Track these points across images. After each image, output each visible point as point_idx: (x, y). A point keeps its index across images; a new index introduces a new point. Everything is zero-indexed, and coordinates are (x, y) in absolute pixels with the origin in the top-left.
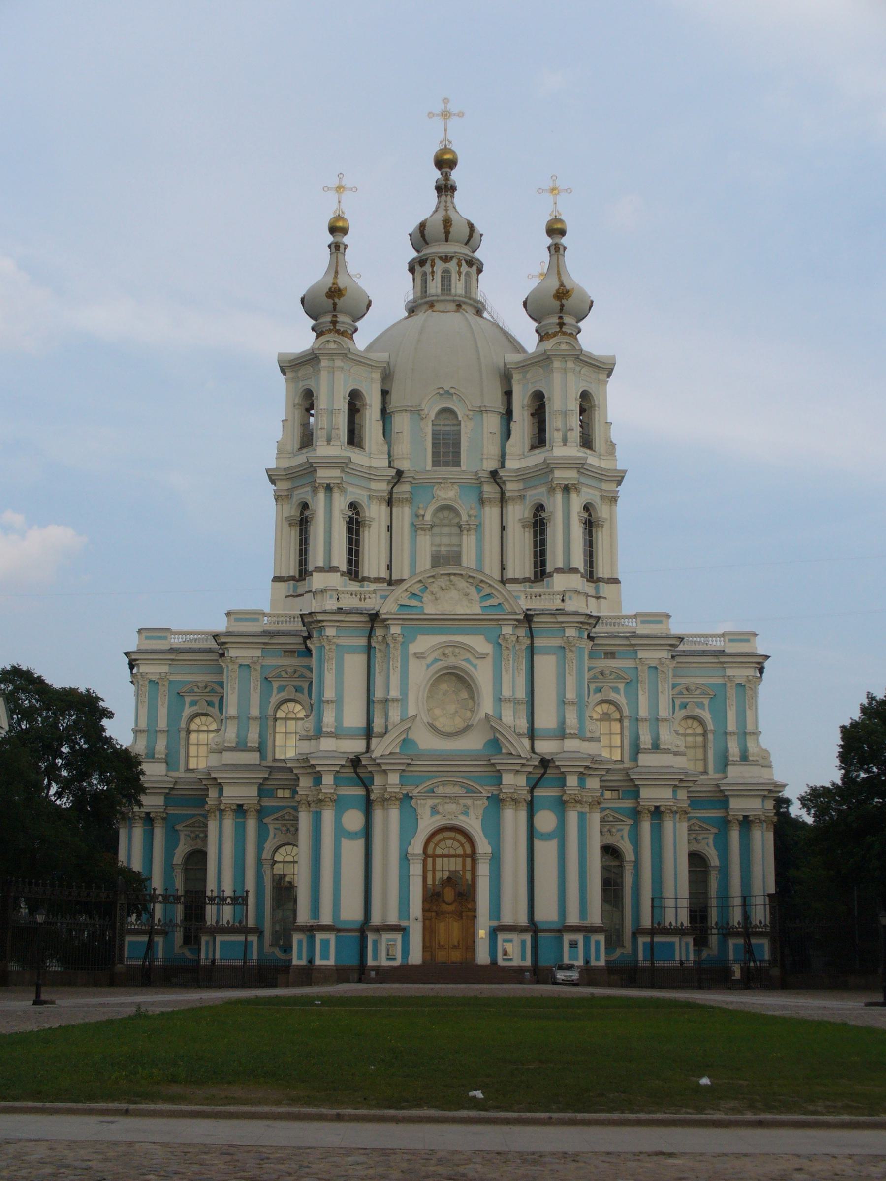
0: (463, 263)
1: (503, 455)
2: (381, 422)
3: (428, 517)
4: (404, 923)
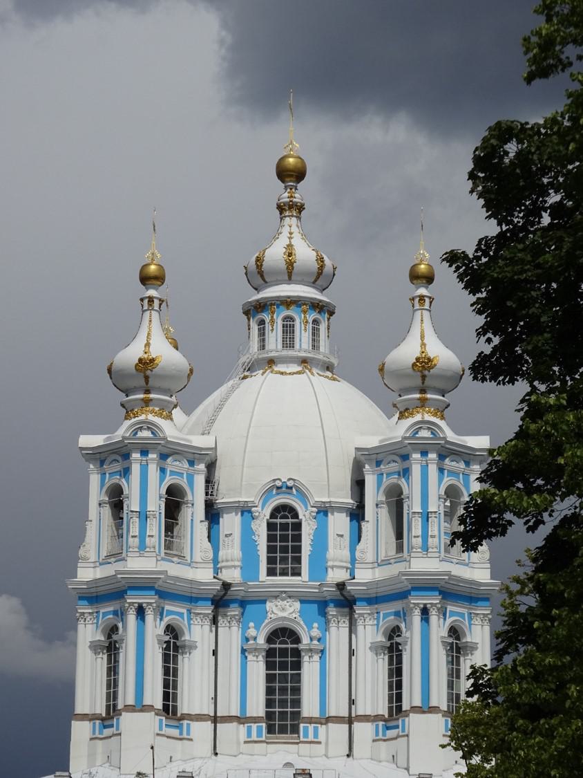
1: (353, 560)
2: (207, 523)
3: (261, 640)
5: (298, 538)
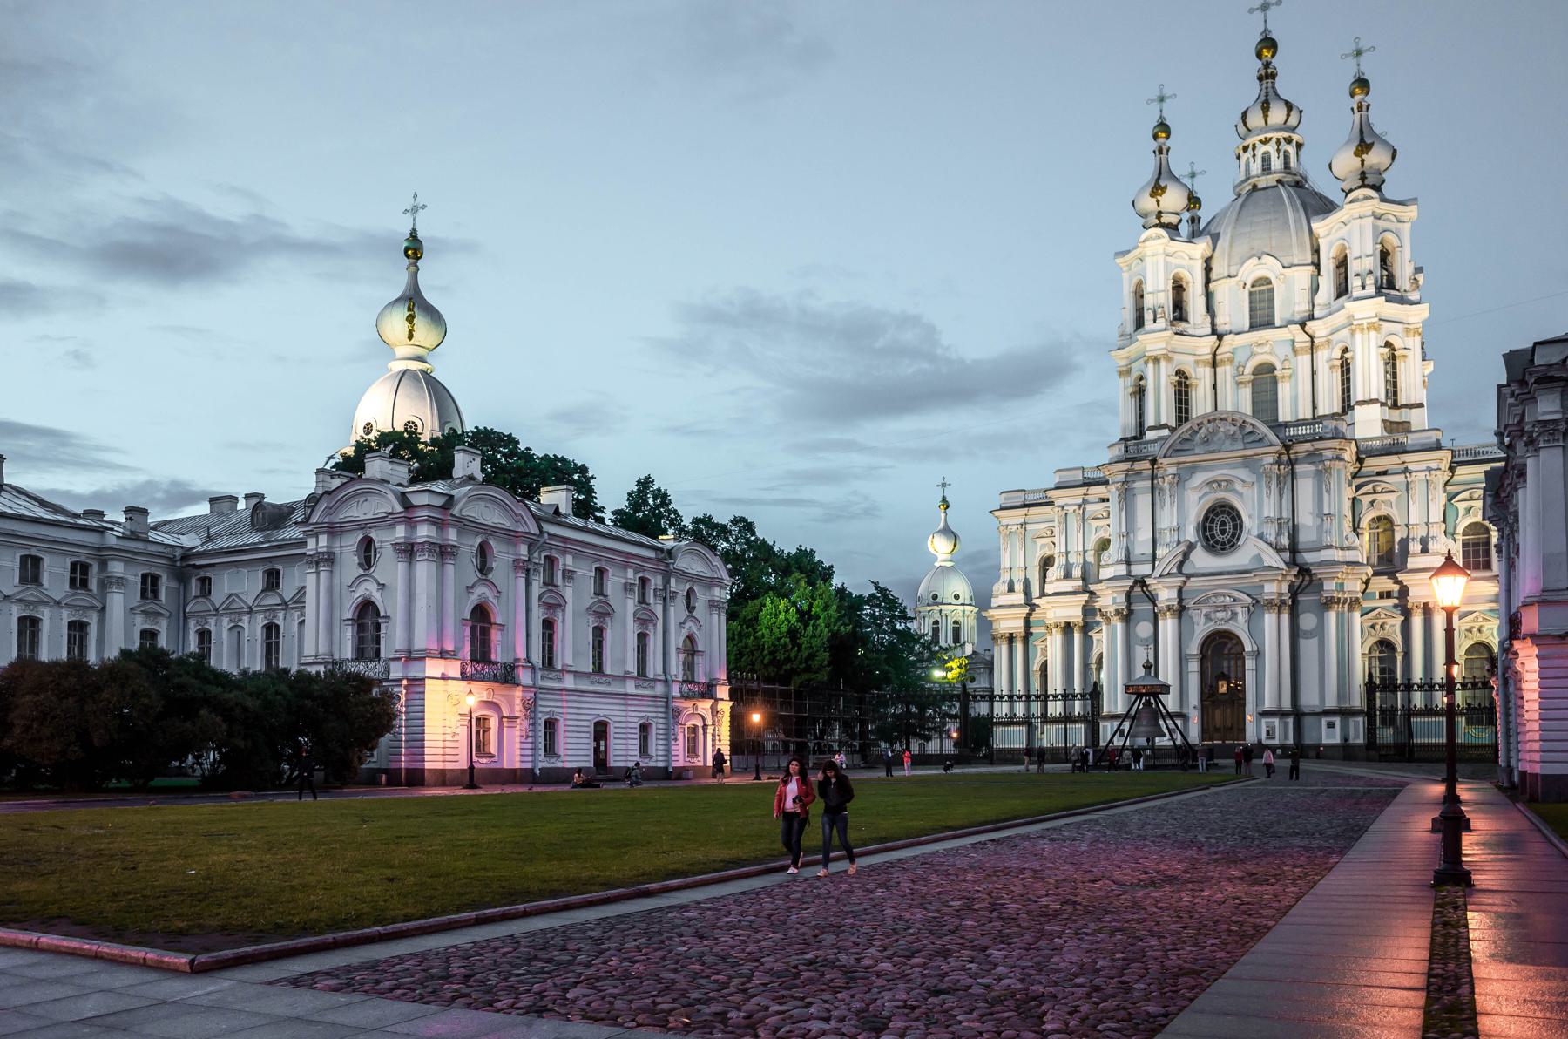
0: (1282, 140)
3: (1249, 369)
4: (1184, 711)
5: (1271, 300)
